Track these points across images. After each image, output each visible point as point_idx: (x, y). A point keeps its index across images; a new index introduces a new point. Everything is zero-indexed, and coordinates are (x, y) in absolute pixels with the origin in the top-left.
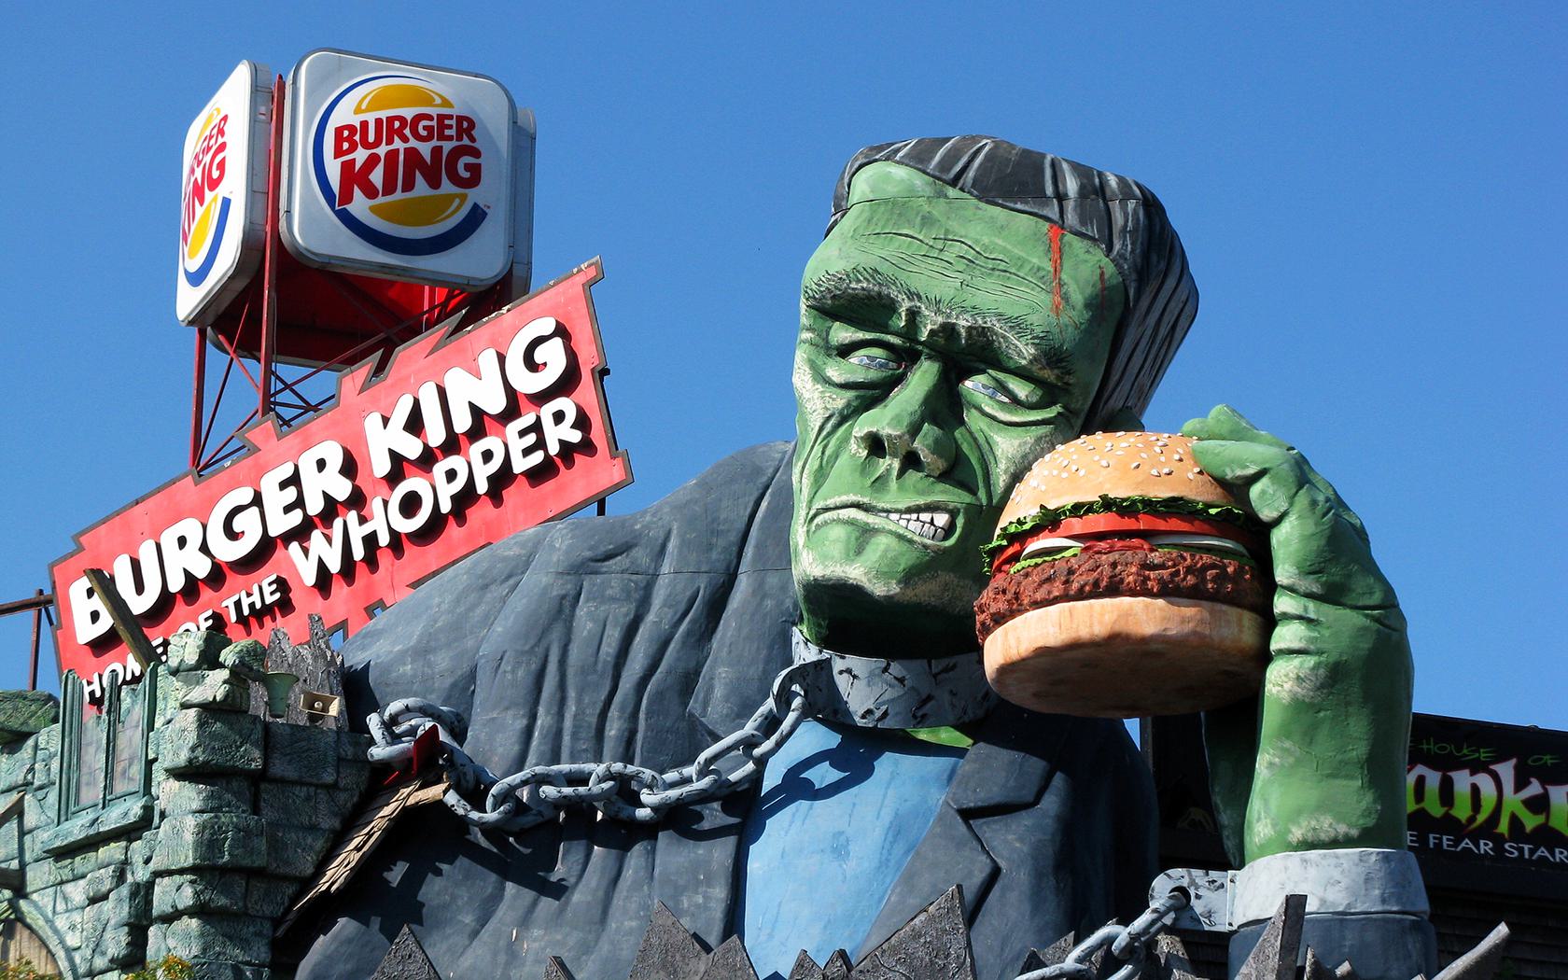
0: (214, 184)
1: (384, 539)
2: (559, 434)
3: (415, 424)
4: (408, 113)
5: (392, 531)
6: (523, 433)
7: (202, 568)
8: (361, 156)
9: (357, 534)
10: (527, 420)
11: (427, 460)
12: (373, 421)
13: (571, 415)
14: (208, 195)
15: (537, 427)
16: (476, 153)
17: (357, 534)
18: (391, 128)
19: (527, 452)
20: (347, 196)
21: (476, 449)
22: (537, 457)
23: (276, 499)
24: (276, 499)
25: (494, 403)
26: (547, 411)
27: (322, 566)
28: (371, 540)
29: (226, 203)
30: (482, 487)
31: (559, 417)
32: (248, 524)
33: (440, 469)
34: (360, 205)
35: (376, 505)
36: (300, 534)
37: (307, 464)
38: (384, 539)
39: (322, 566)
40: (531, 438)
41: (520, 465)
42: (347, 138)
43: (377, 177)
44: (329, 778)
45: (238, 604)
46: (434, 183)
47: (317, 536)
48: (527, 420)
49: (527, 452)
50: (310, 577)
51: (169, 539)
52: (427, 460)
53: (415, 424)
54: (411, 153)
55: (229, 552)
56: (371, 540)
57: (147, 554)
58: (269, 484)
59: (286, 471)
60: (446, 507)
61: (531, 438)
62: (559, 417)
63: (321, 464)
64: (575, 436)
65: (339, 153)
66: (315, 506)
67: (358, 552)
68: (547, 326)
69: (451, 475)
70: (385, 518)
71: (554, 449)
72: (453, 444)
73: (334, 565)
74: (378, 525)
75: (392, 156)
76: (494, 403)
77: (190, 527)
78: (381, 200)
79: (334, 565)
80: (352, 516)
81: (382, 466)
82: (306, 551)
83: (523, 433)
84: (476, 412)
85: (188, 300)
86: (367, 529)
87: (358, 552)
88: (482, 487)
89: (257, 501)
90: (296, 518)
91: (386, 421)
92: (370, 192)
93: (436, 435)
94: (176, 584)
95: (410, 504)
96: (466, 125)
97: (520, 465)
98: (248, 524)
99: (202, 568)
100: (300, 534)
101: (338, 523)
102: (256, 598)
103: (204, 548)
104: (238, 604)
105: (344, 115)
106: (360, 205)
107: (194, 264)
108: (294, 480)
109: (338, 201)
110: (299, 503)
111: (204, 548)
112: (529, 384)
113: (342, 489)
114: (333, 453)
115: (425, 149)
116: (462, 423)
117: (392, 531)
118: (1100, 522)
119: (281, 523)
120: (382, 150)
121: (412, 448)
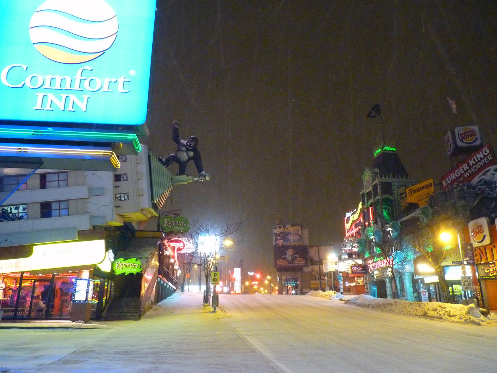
0: (449, 142)
1: (473, 172)
2: (490, 159)
3: (474, 160)
4: (467, 131)
5: (474, 171)
6: (486, 159)
7: (455, 178)
8: (463, 136)
9: (470, 172)
10: (487, 157)
11: (476, 163)
12: (470, 161)
13: (491, 156)
14: (449, 143)
15: (487, 158)
16: (475, 133)
17: (470, 172)
18: (466, 133)
19: (487, 161)
20: (463, 140)
21: (481, 162)
22: (488, 161)
23: (461, 170)
24: (461, 170)
25: (482, 156)
26: (488, 156)
27: (467, 175)
28: (472, 172)
29: (451, 144)
30: (483, 165)
31: (490, 157)
32: (459, 173)
34: (464, 140)
35: (472, 168)
36: (465, 173)
38: (473, 172)
39: (467, 175)
40: (487, 159)
41: (486, 162)
42: (461, 135)
43: (465, 137)
44: (472, 195)
45: (460, 180)
46: (471, 136)
47: (466, 173)
48: (487, 157)
49: (487, 161)
50: (466, 176)
51: (451, 176)
52: (476, 163)
53: (474, 160)
54: (469, 134)
55: (458, 176)
56: (472, 172)
57: (449, 177)
59: (462, 167)
60: (479, 167)
61: (487, 159)
62: (490, 157)
63: (465, 166)
64: (492, 158)
65: (461, 136)
66: (465, 170)
67: (471, 173)
69: (479, 165)
70: (473, 170)
71: (490, 160)
72: (479, 161)
73: (468, 174)
74: (472, 170)
75: (466, 135)
76: (482, 156)
77: (453, 174)
78: (466, 139)
80: (469, 170)
81: (471, 165)
82: (465, 174)
83: (486, 159)
84: (480, 158)
85: (449, 153)
86: (471, 171)
87: (471, 173)
88: (483, 165)
89: (459, 171)
91: (471, 161)
92: (465, 139)
94: (453, 180)
95: (475, 168)
96: (474, 130)
97: (486, 162)
98: (459, 173)
99: (455, 178)
100: (465, 173)
101: (468, 171)
102: (461, 179)
103: (455, 176)
104: (460, 180)
105: (461, 132)
106: (464, 140)
107: (449, 150)
108: (463, 168)
109: (461, 141)
110: (464, 170)
111: (455, 176)
112: (486, 154)
113: (468, 168)
114: (466, 165)
115: (470, 134)
116: (479, 159)
117: (474, 171)
119: (462, 172)
120: (465, 135)
121: (474, 163)
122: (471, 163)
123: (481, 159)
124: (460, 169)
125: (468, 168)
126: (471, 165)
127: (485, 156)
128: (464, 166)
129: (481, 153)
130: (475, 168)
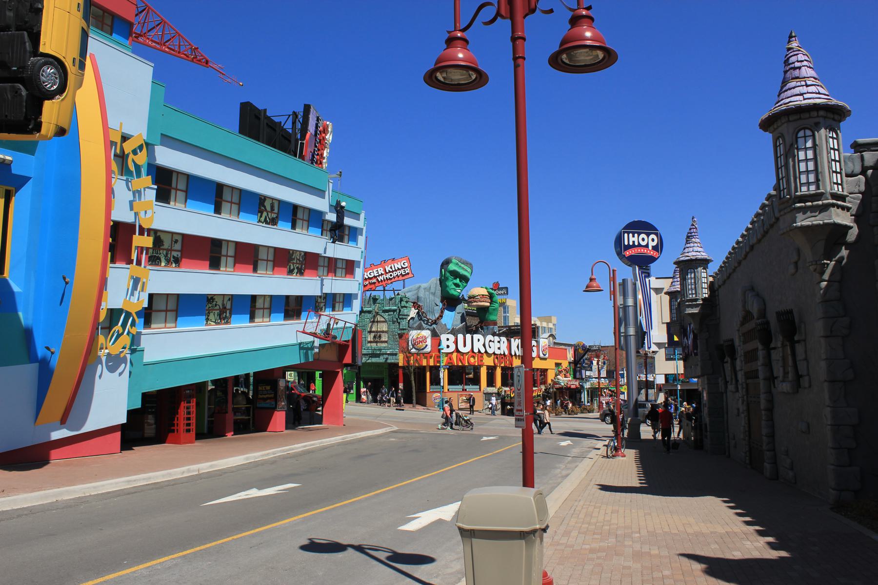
3: (391, 268)
11: (393, 271)
12: (386, 267)
21: (398, 271)
23: (375, 272)
24: (375, 272)
26: (406, 269)
28: (386, 278)
32: (372, 274)
33: (394, 273)
36: (379, 276)
37: (379, 269)
52: (393, 271)
58: (375, 270)
59: (376, 270)
68: (406, 261)
70: (388, 276)
72: (396, 270)
73: (383, 280)
74: (387, 276)
76: (400, 268)
79: (383, 280)
81: (387, 271)
90: (378, 274)
93: (394, 269)
95: (391, 275)
97: (403, 274)
100: (379, 276)
110: (378, 273)
116: (397, 269)
118: (481, 296)
121: (391, 270)
122: (388, 269)
123: (399, 269)
124: (375, 270)
125: (383, 273)
126: (387, 271)
127: (402, 268)
128: (379, 269)
129: (399, 263)
130: (391, 275)
